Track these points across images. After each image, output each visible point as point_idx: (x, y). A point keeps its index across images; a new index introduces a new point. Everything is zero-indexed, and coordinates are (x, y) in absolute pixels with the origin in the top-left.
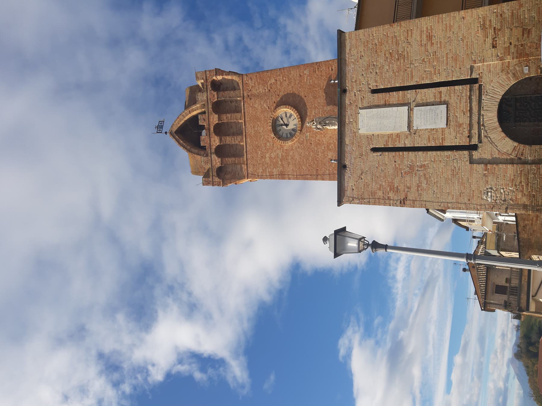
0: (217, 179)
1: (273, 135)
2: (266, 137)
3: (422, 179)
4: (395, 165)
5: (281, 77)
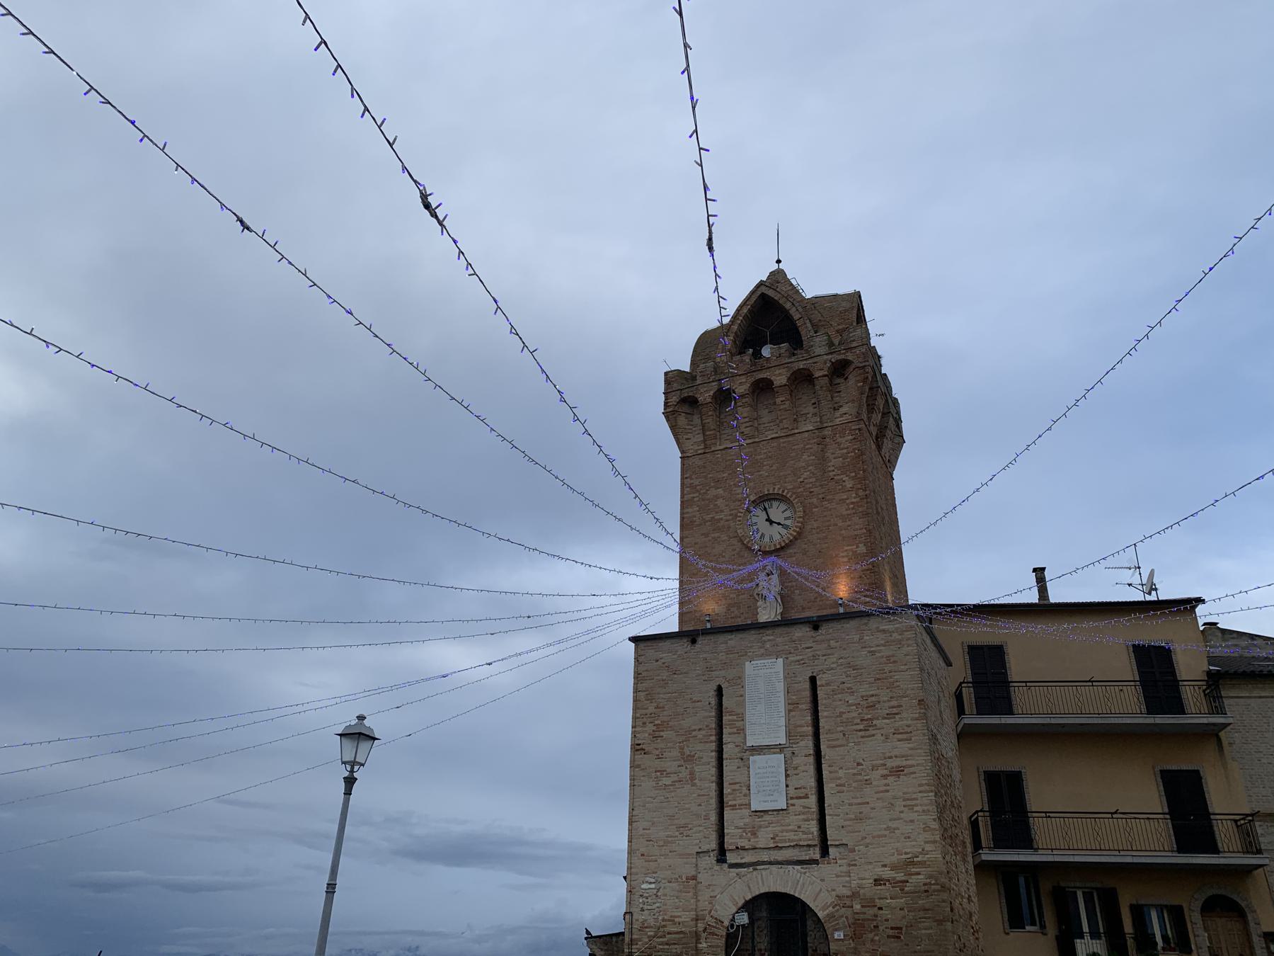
0: (674, 399)
3: (674, 777)
4: (695, 730)
5: (853, 500)
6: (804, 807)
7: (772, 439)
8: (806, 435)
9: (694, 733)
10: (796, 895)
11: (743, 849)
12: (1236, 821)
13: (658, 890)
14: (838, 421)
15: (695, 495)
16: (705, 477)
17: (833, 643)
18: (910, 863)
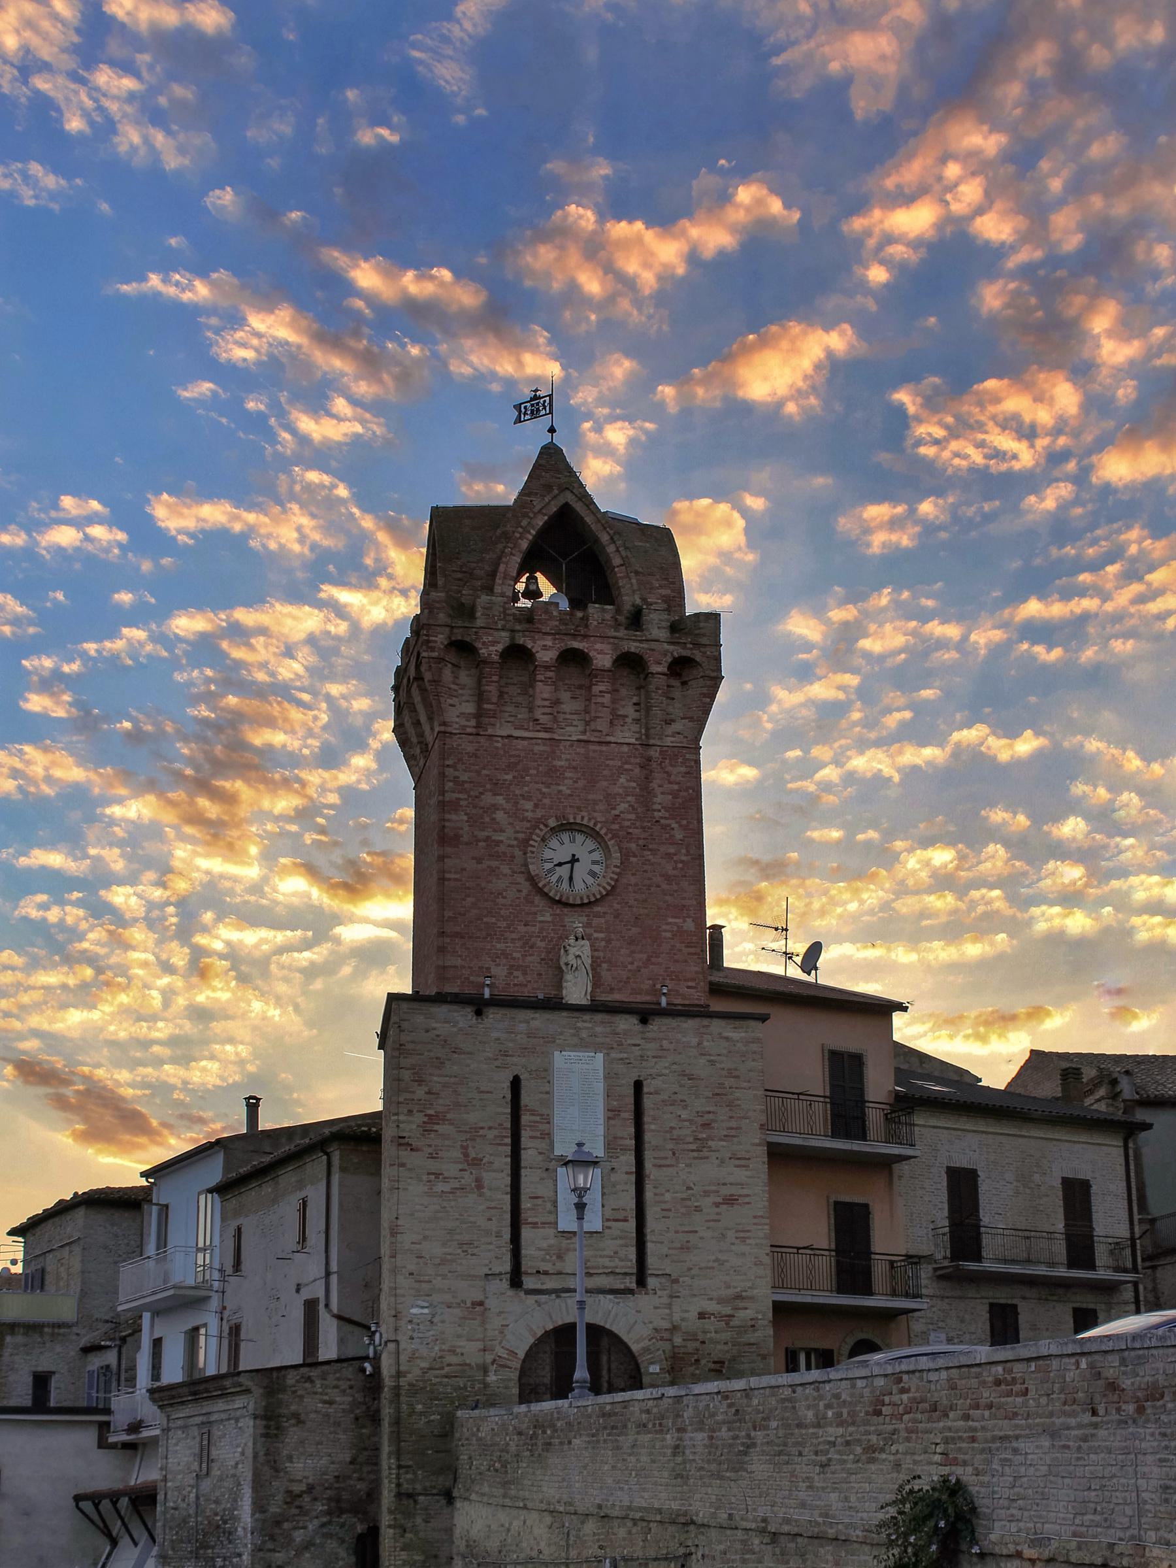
1: (552, 823)
2: (547, 801)
4: (482, 1128)
5: (684, 858)
6: (622, 1231)
7: (579, 741)
8: (625, 749)
9: (481, 1132)
10: (607, 1326)
11: (546, 1273)
12: (892, 1263)
13: (434, 1316)
14: (668, 741)
15: (461, 796)
16: (478, 773)
17: (665, 1043)
18: (739, 1297)
